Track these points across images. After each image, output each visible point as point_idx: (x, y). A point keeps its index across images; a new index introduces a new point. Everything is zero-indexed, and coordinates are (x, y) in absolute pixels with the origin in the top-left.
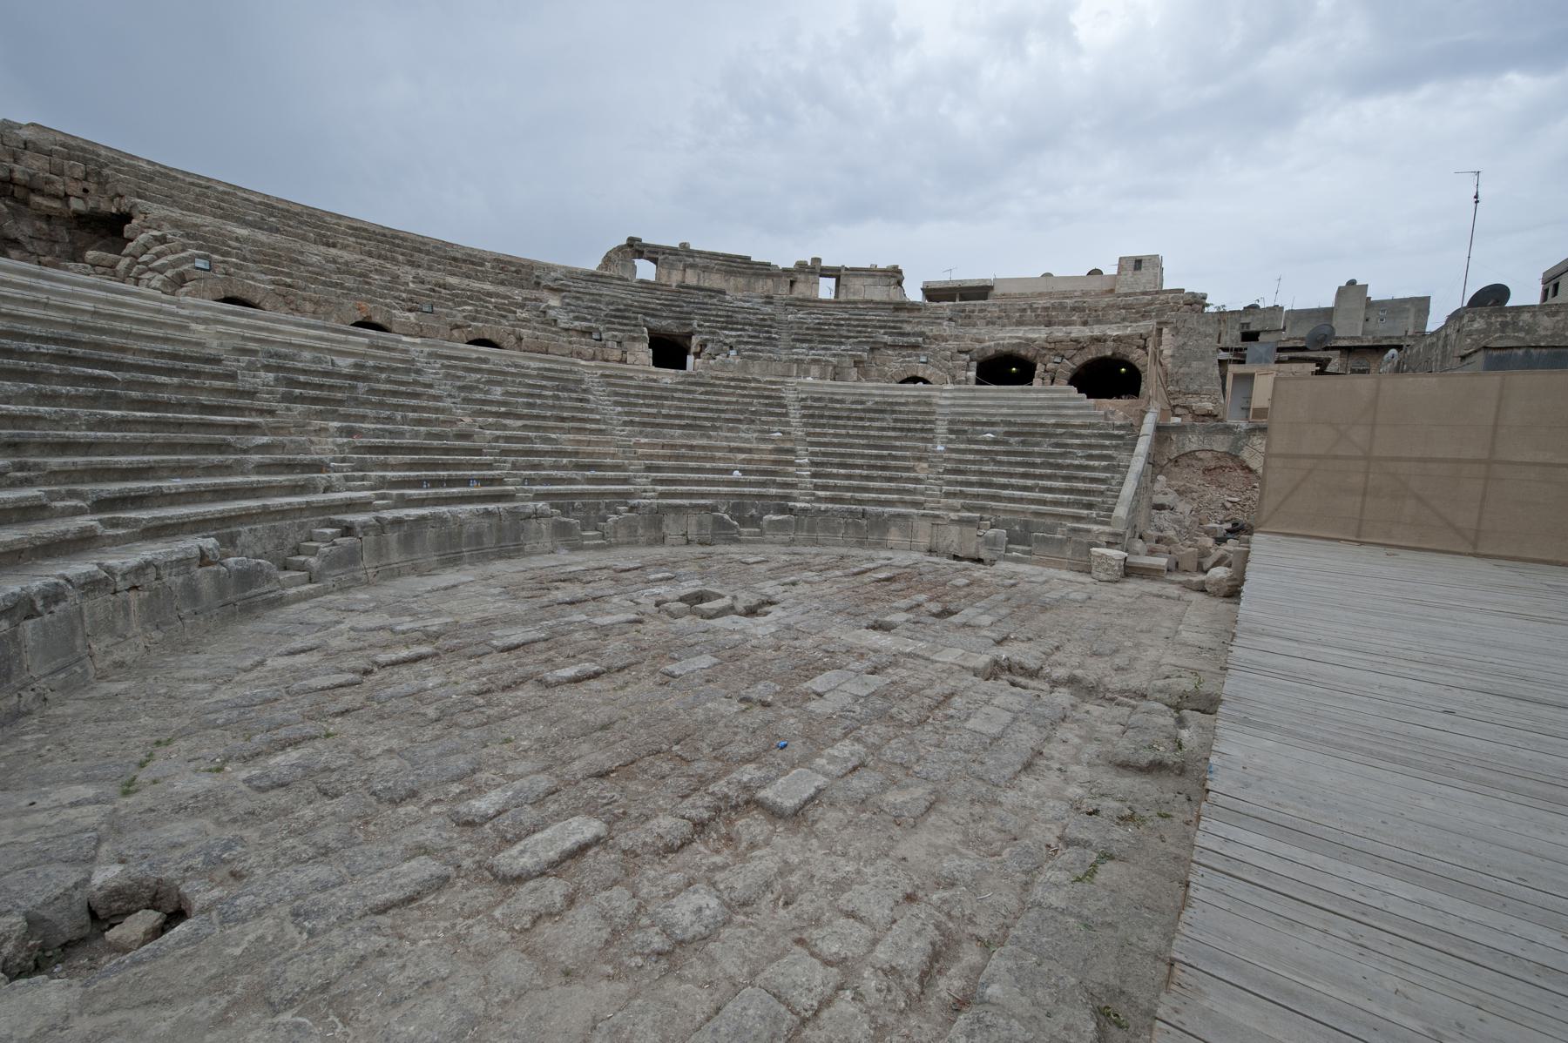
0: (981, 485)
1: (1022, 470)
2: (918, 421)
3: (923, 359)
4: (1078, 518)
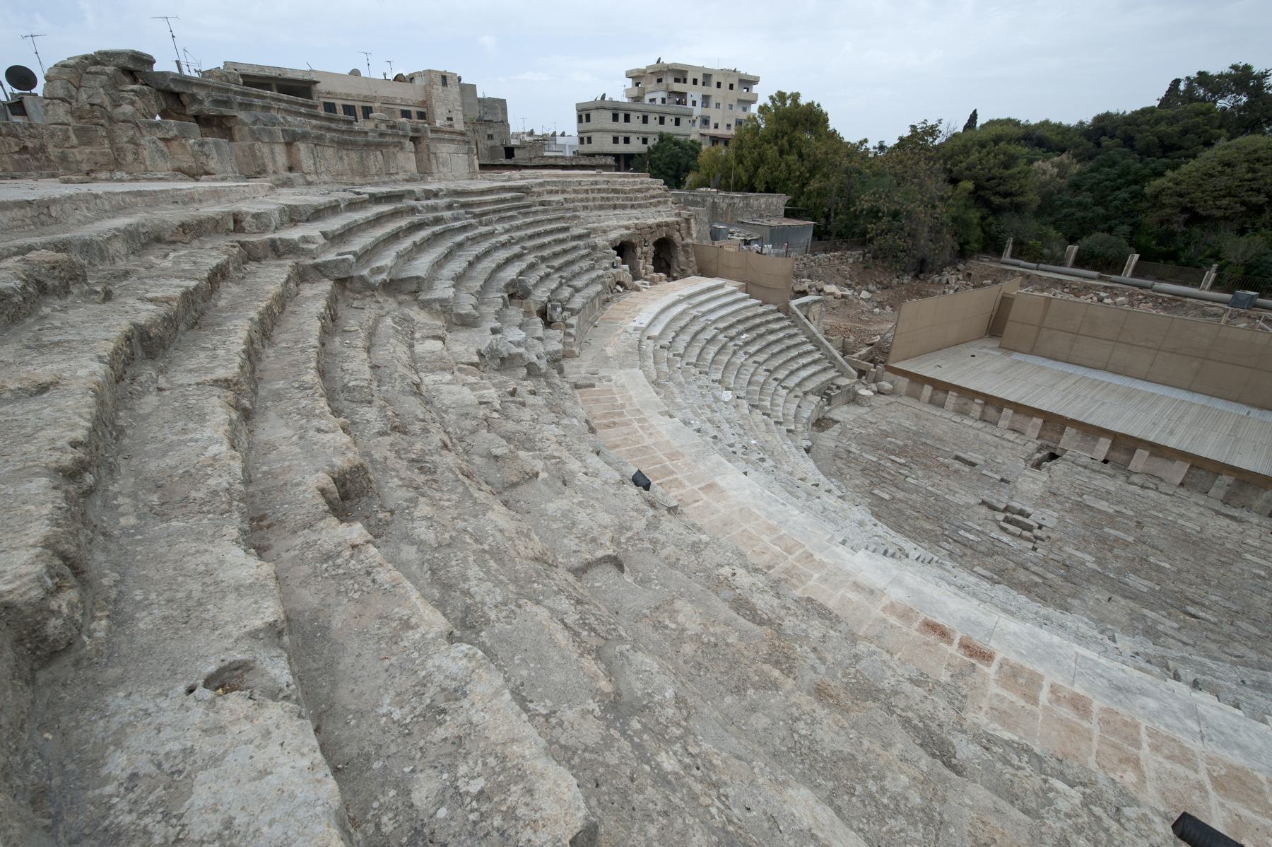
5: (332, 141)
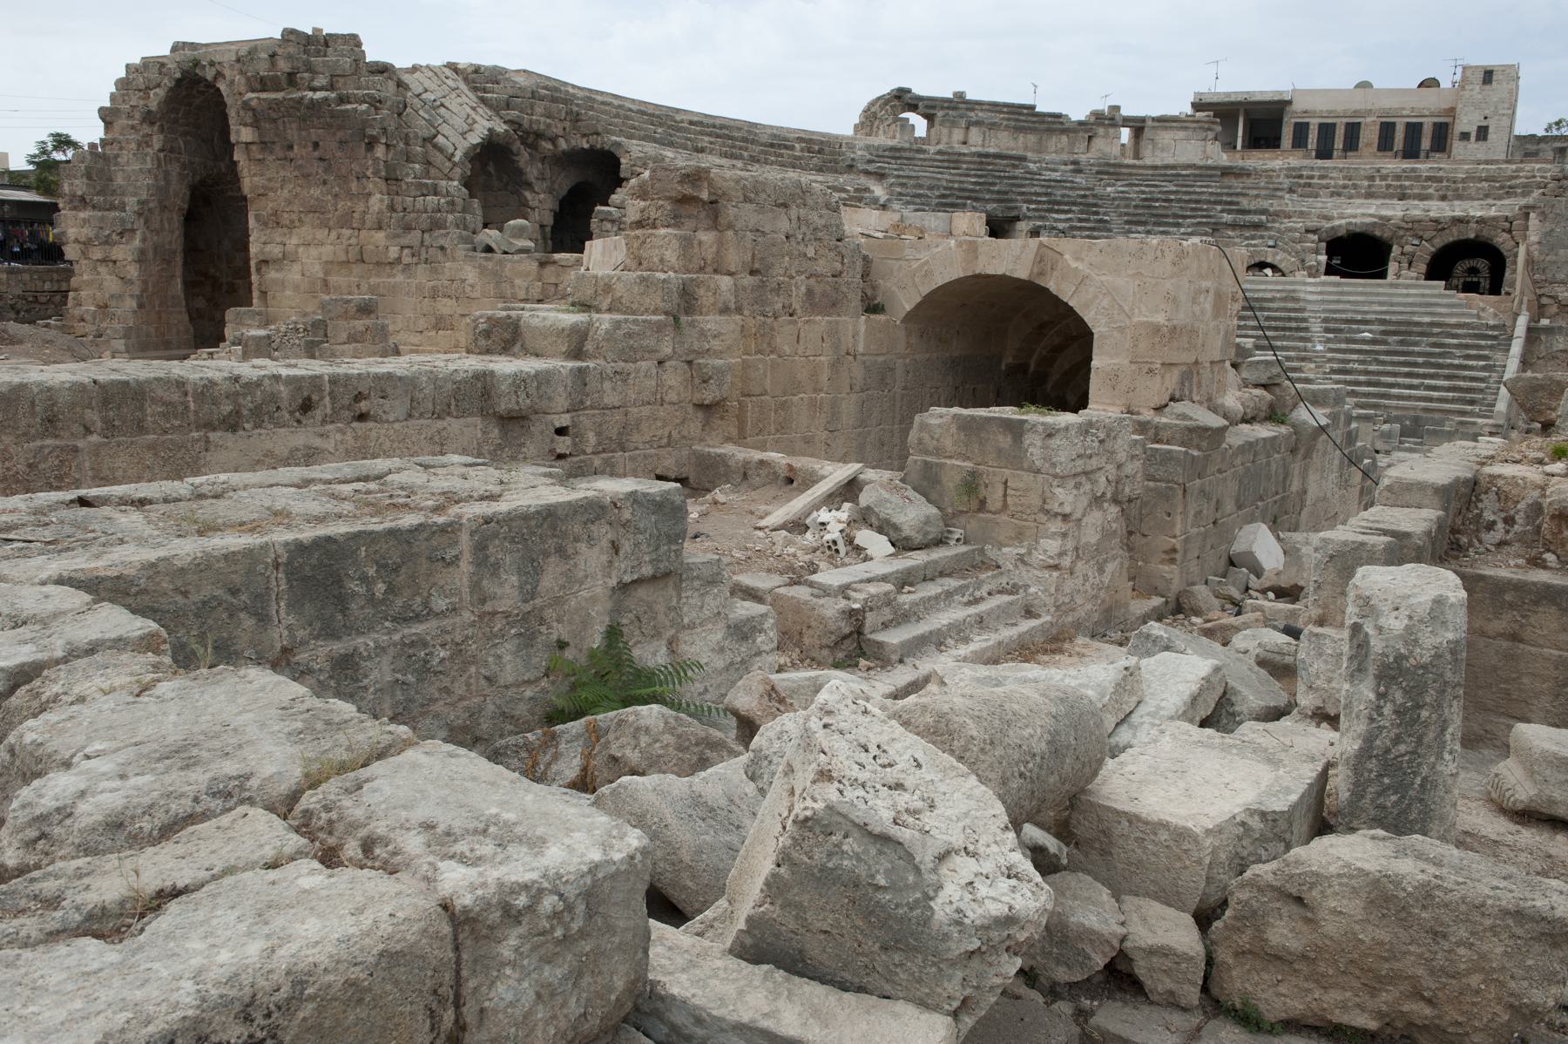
0: (1369, 384)
1: (1407, 369)
2: (1290, 319)
3: (1271, 243)
4: (1463, 413)
5: (1006, 126)
